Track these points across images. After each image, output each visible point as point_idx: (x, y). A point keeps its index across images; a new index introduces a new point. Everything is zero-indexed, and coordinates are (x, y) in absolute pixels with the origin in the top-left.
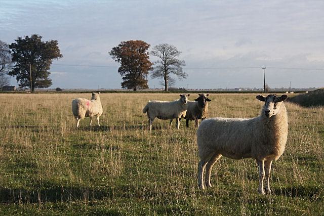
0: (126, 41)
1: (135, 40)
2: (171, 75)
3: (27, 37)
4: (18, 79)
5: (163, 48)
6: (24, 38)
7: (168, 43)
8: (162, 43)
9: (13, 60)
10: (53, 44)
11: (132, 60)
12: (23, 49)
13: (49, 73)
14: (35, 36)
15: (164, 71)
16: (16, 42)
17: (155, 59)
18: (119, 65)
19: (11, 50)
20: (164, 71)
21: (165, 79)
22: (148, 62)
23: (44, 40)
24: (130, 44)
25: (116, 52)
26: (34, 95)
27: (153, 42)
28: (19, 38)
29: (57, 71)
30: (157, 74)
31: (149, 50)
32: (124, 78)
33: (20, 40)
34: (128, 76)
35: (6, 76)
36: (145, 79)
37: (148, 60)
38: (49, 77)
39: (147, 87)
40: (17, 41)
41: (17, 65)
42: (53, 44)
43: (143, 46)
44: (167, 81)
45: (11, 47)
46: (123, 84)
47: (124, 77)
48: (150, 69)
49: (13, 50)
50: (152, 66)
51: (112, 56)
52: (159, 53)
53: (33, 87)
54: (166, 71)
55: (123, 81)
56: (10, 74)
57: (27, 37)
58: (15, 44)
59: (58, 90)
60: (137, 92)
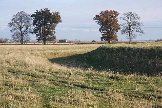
0: (104, 11)
1: (110, 10)
2: (134, 33)
3: (42, 10)
4: (37, 36)
5: (129, 15)
6: (39, 11)
7: (23, 11)
8: (128, 11)
9: (34, 24)
10: (56, 14)
11: (107, 22)
12: (39, 18)
13: (54, 32)
14: (47, 9)
15: (129, 30)
16: (35, 13)
17: (122, 22)
18: (100, 27)
19: (33, 18)
20: (129, 30)
21: (130, 35)
22: (117, 24)
23: (52, 12)
24: (105, 13)
25: (97, 18)
26: (45, 45)
27: (122, 11)
28: (37, 11)
29: (59, 31)
30: (124, 32)
31: (119, 17)
32: (102, 35)
33: (37, 12)
34: (105, 34)
35: (30, 34)
36: (116, 35)
37: (118, 23)
38: (55, 35)
39: (117, 40)
40: (36, 13)
41: (36, 28)
42: (56, 14)
43: (115, 14)
44: (131, 36)
45: (32, 16)
46: (102, 38)
47: (102, 34)
48: (119, 29)
49: (34, 18)
50: (120, 27)
51: (95, 21)
52: (126, 18)
53: (45, 41)
54: (130, 29)
55: (101, 36)
56: (32, 33)
57: (42, 10)
58: (35, 14)
59: (63, 41)
60: (46, 45)
